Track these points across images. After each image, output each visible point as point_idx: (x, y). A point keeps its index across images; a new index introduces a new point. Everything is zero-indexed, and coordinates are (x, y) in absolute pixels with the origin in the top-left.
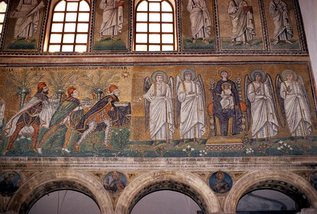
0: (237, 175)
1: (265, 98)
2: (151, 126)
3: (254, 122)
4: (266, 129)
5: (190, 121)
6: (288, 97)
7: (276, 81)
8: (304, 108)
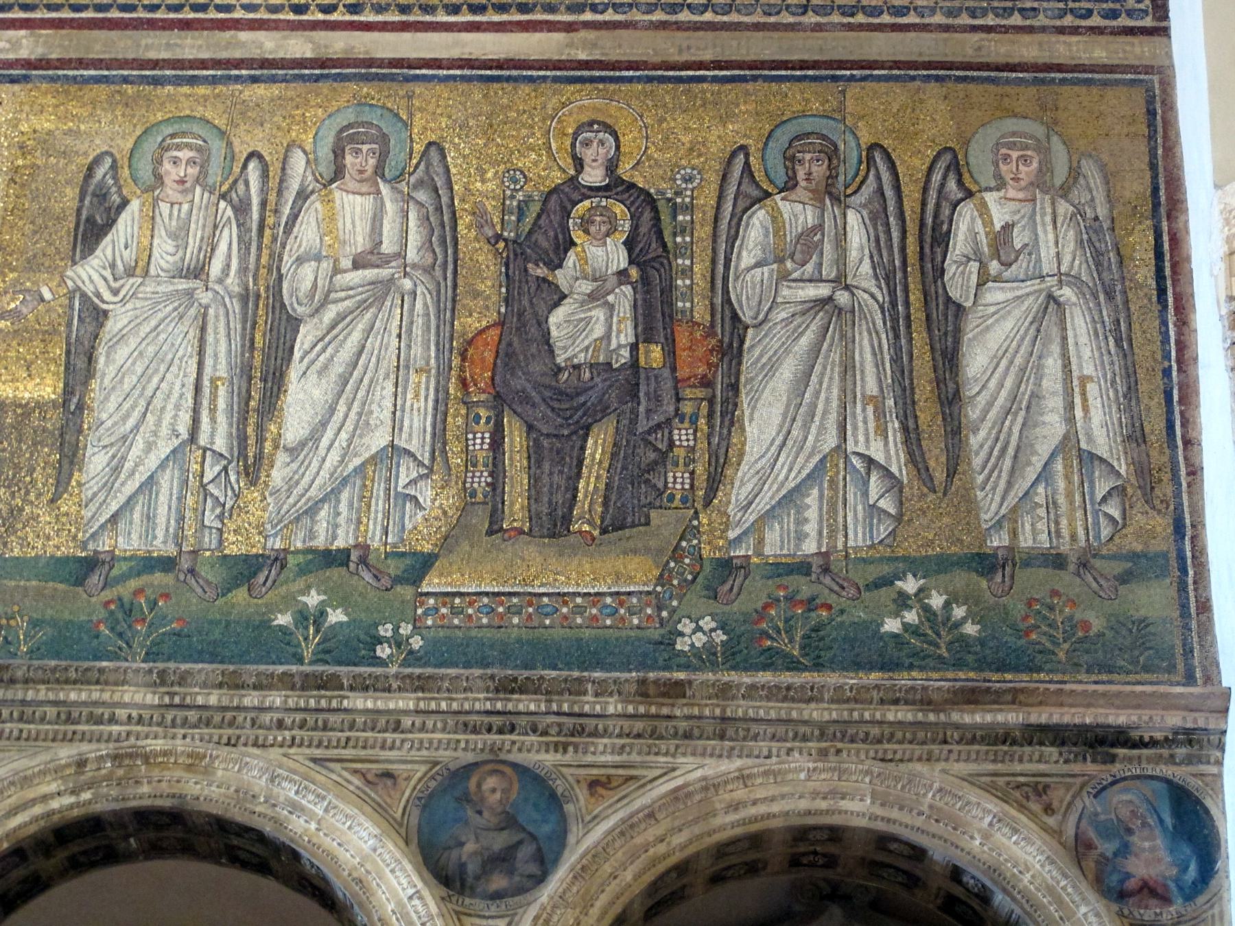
0: (600, 790)
1: (843, 298)
2: (96, 462)
3: (753, 450)
4: (821, 496)
5: (344, 435)
6: (995, 295)
7: (925, 190)
8: (1089, 370)
